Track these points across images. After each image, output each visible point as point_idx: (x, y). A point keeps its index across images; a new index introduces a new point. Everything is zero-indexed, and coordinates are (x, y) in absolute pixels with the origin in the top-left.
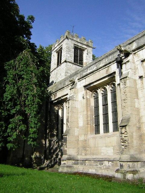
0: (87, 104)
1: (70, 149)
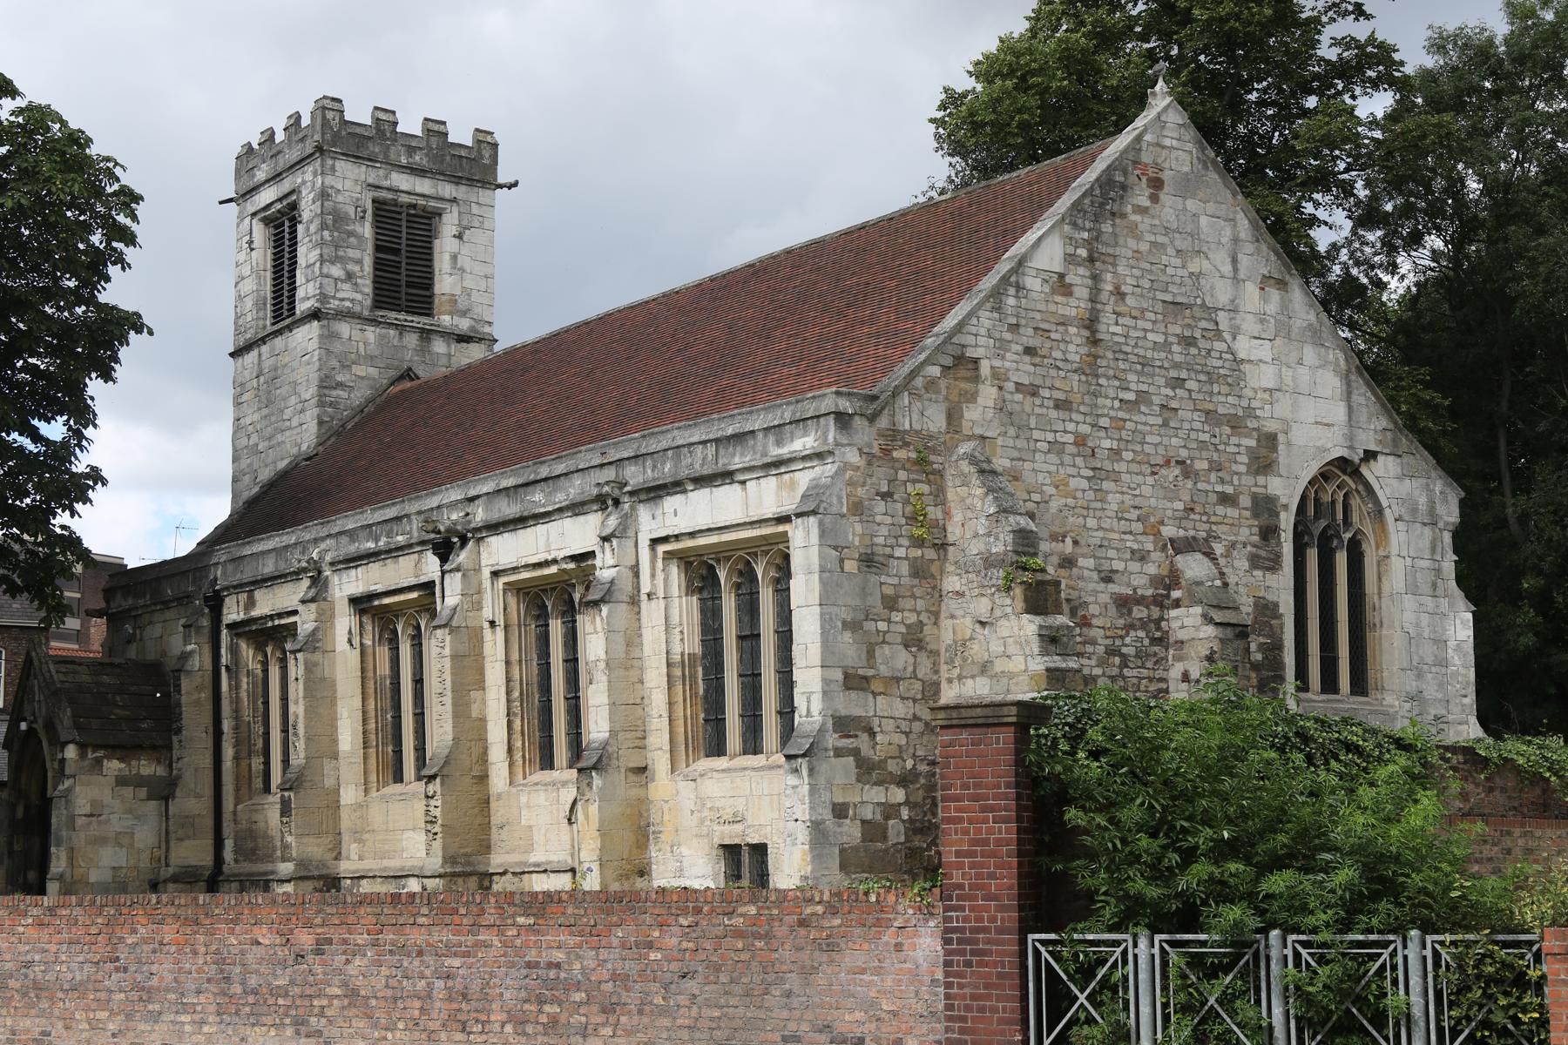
0: (363, 670)
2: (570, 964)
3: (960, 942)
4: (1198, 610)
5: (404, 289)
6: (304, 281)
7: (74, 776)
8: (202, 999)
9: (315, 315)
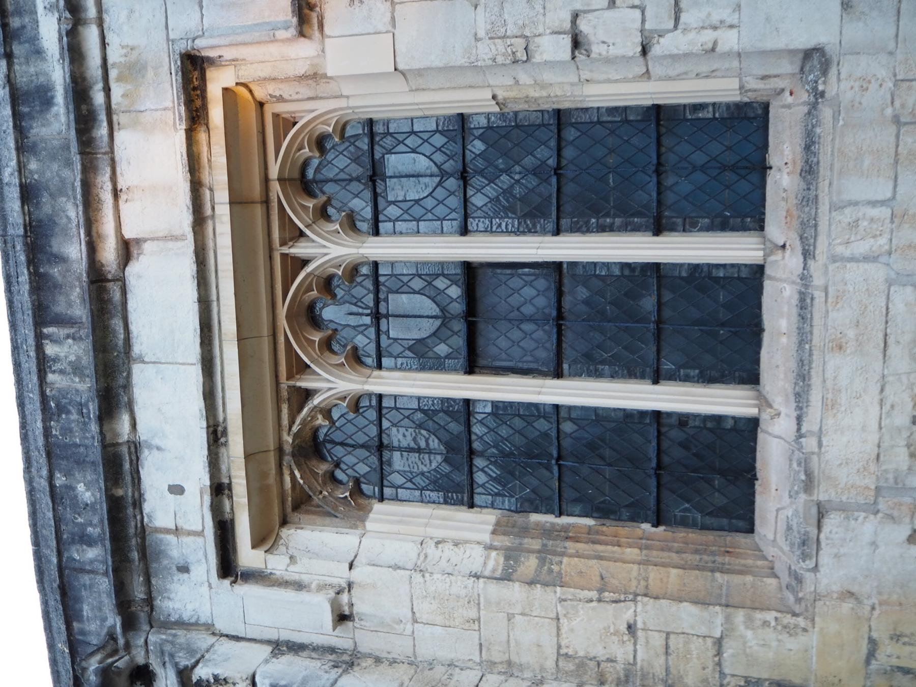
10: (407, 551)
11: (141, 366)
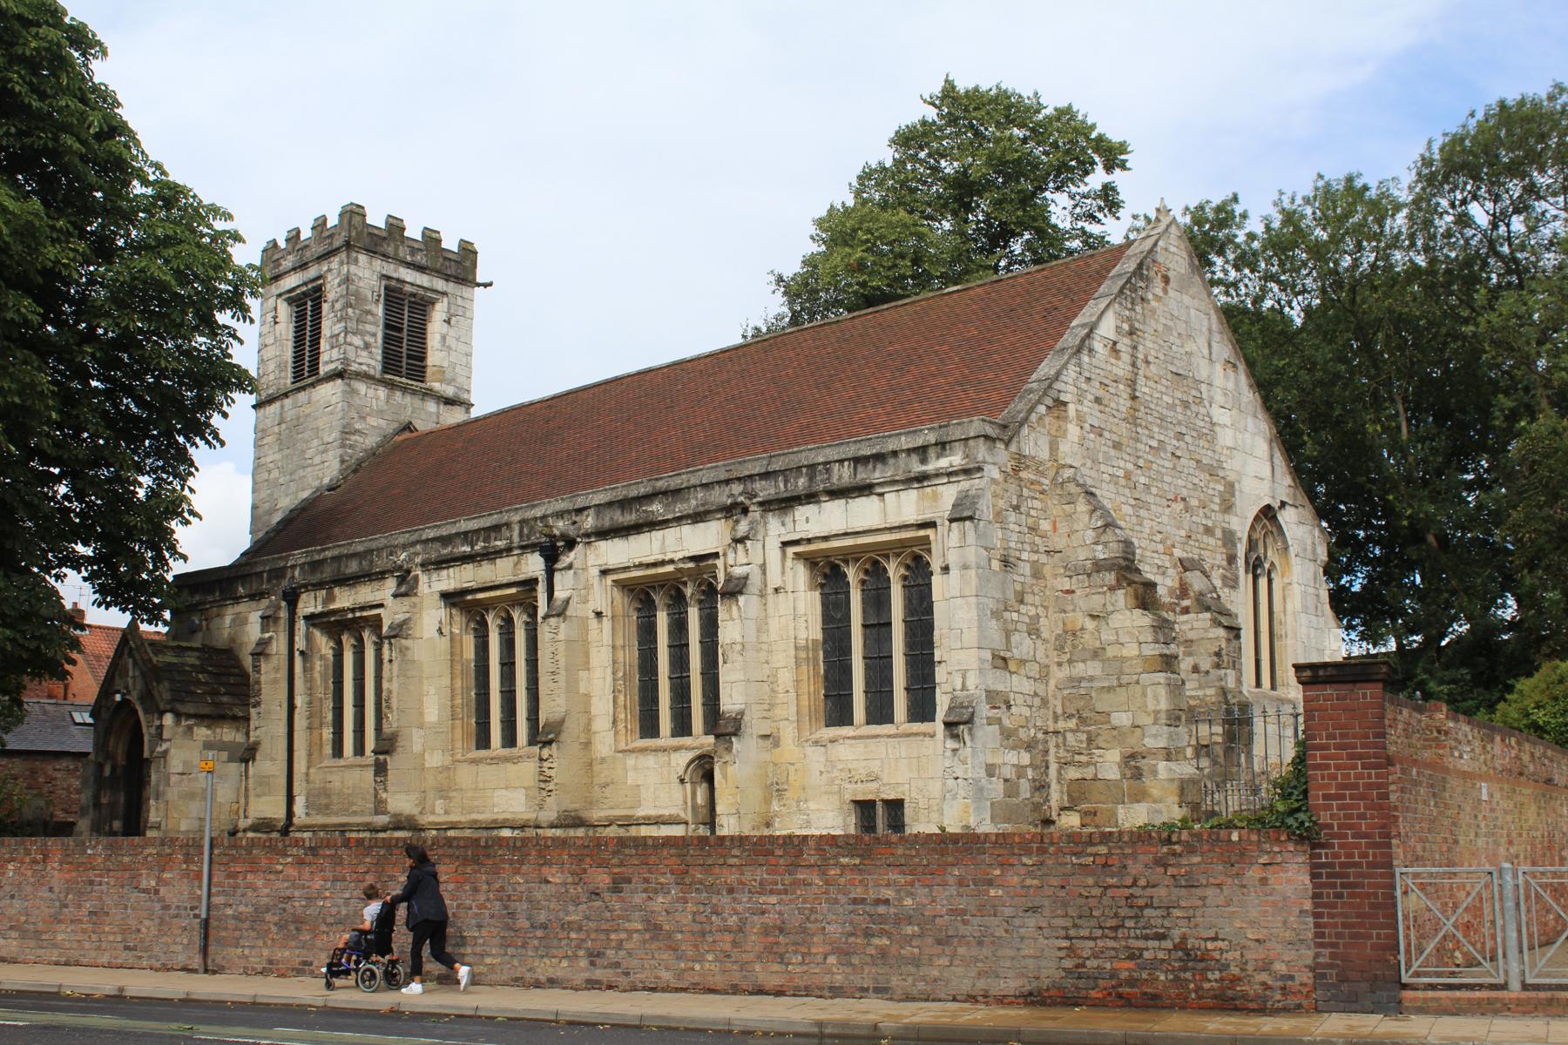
0: (452, 654)
1: (398, 796)
2: (900, 900)
3: (1329, 875)
4: (1208, 615)
5: (404, 360)
6: (328, 347)
7: (169, 740)
8: (484, 932)
9: (339, 375)
10: (801, 609)
11: (843, 507)
